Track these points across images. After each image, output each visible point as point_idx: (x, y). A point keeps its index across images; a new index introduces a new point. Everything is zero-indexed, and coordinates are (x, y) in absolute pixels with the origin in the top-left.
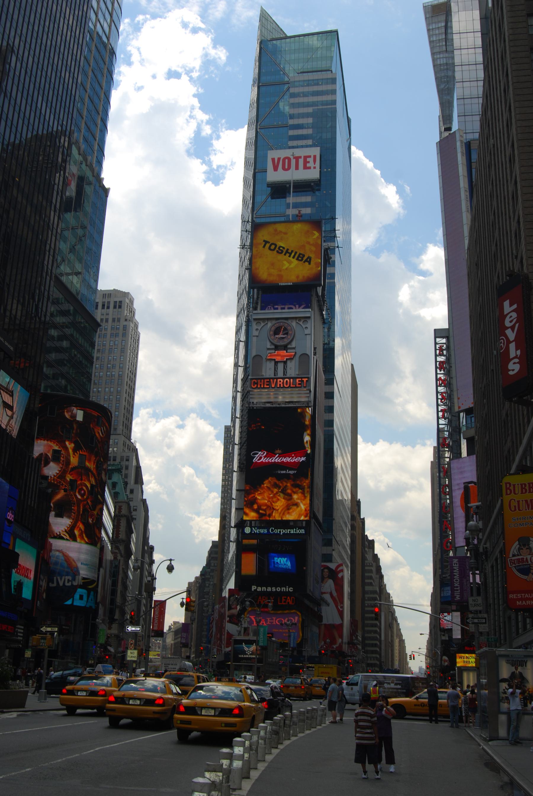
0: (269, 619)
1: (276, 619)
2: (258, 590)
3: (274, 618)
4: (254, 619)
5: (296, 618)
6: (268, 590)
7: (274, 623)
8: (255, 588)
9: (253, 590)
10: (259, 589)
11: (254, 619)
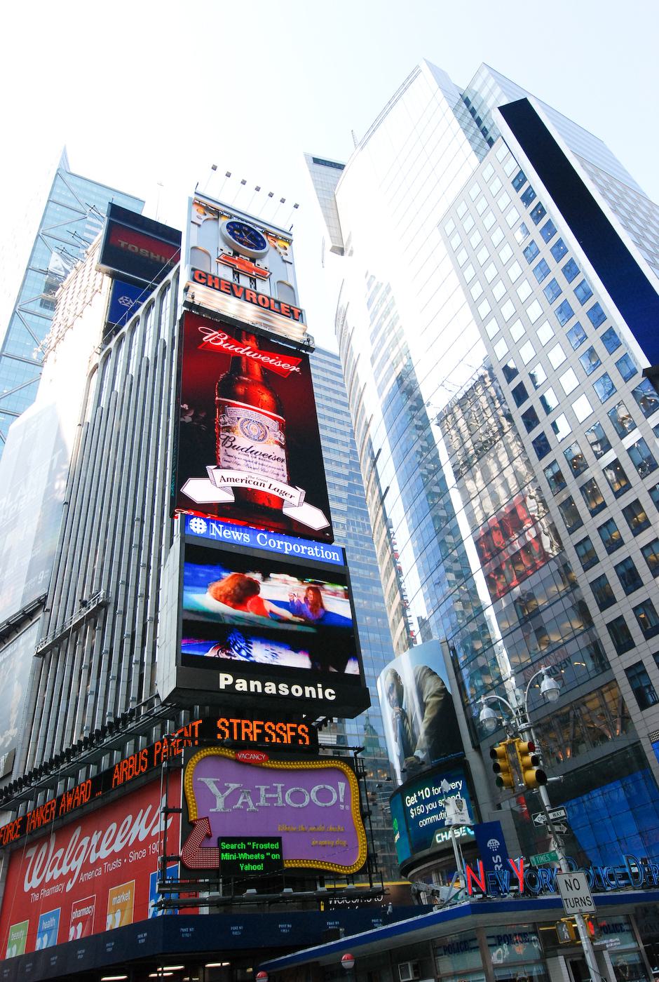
0: (263, 788)
1: (284, 791)
2: (238, 687)
3: (280, 786)
4: (214, 789)
5: (342, 785)
6: (267, 690)
7: (280, 803)
8: (230, 681)
9: (222, 686)
10: (241, 685)
11: (214, 789)
